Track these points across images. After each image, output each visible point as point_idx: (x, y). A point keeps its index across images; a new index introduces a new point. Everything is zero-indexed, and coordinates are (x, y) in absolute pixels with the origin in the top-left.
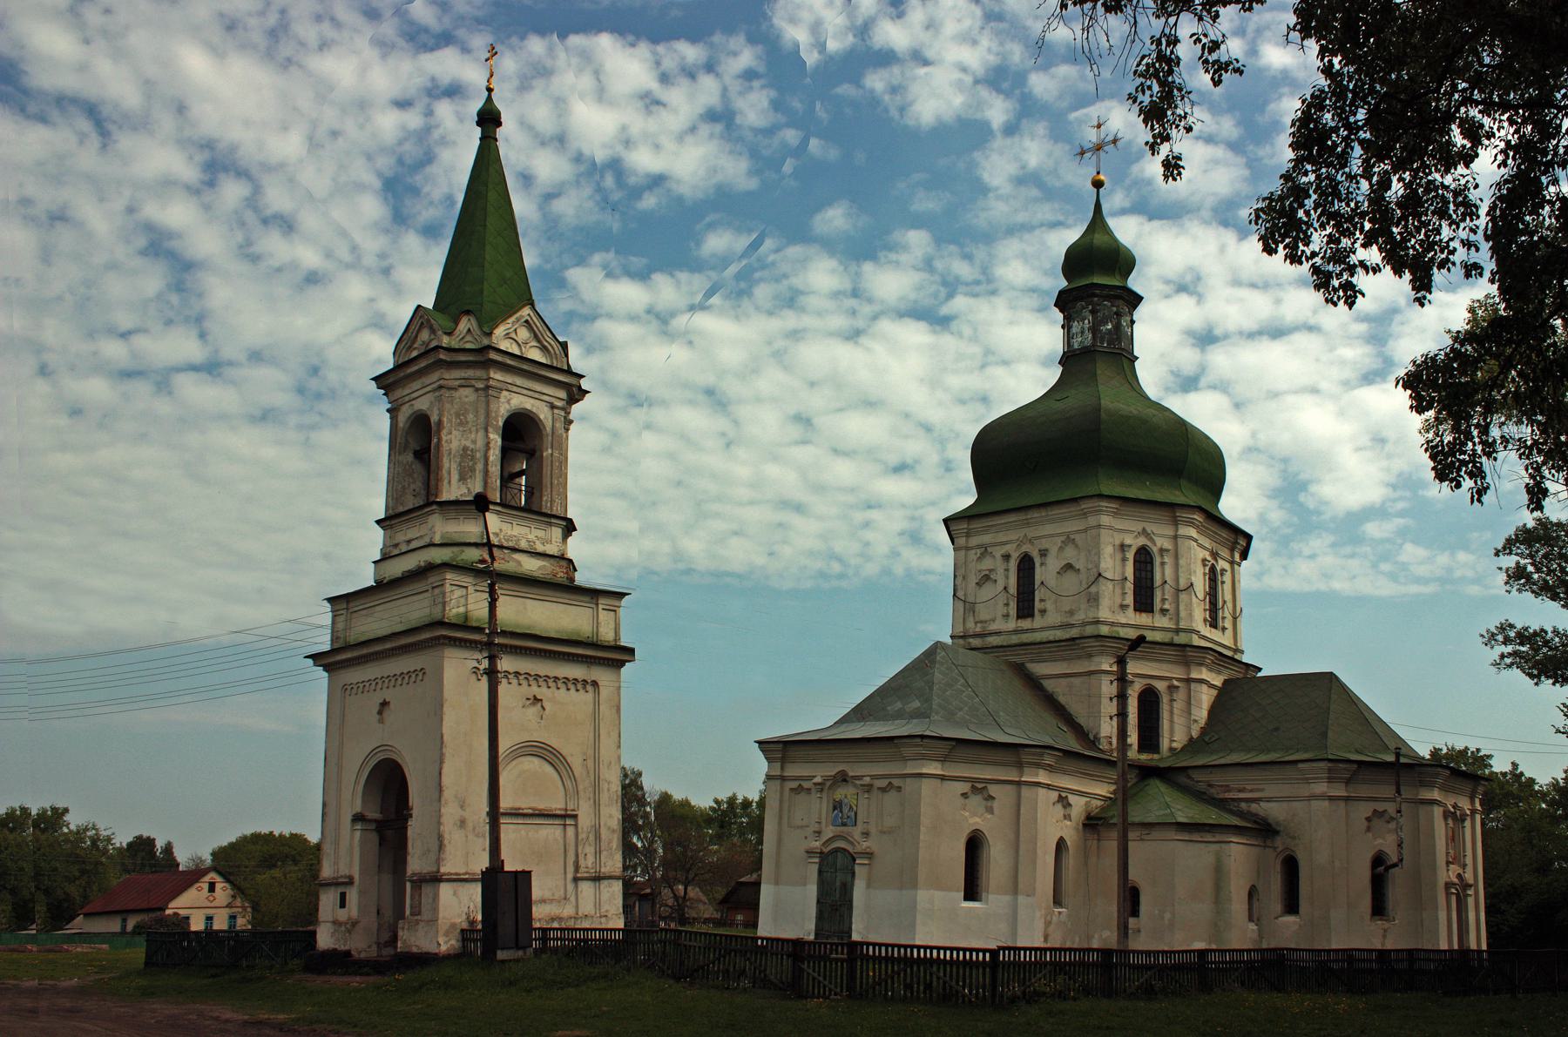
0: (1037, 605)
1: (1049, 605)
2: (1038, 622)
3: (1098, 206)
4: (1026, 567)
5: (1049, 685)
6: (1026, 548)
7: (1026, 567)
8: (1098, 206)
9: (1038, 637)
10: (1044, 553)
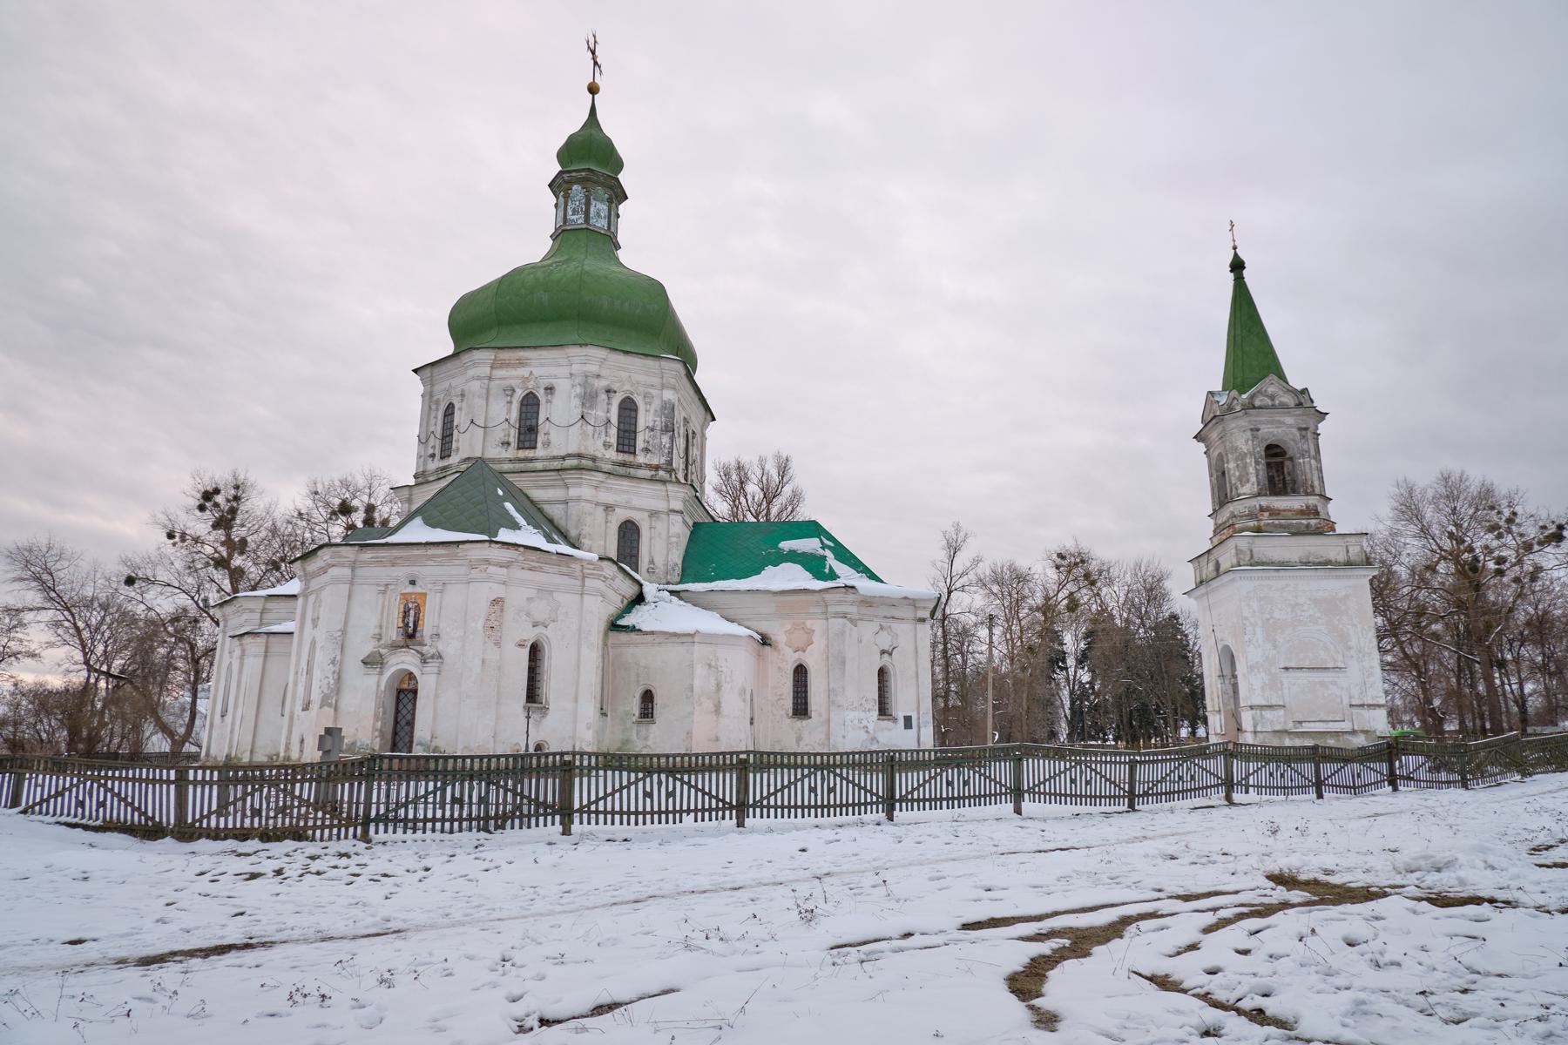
0: (541, 439)
1: (553, 437)
2: (540, 452)
3: (593, 109)
4: (530, 405)
5: (556, 511)
6: (531, 385)
7: (530, 405)
8: (593, 109)
9: (539, 465)
10: (550, 390)
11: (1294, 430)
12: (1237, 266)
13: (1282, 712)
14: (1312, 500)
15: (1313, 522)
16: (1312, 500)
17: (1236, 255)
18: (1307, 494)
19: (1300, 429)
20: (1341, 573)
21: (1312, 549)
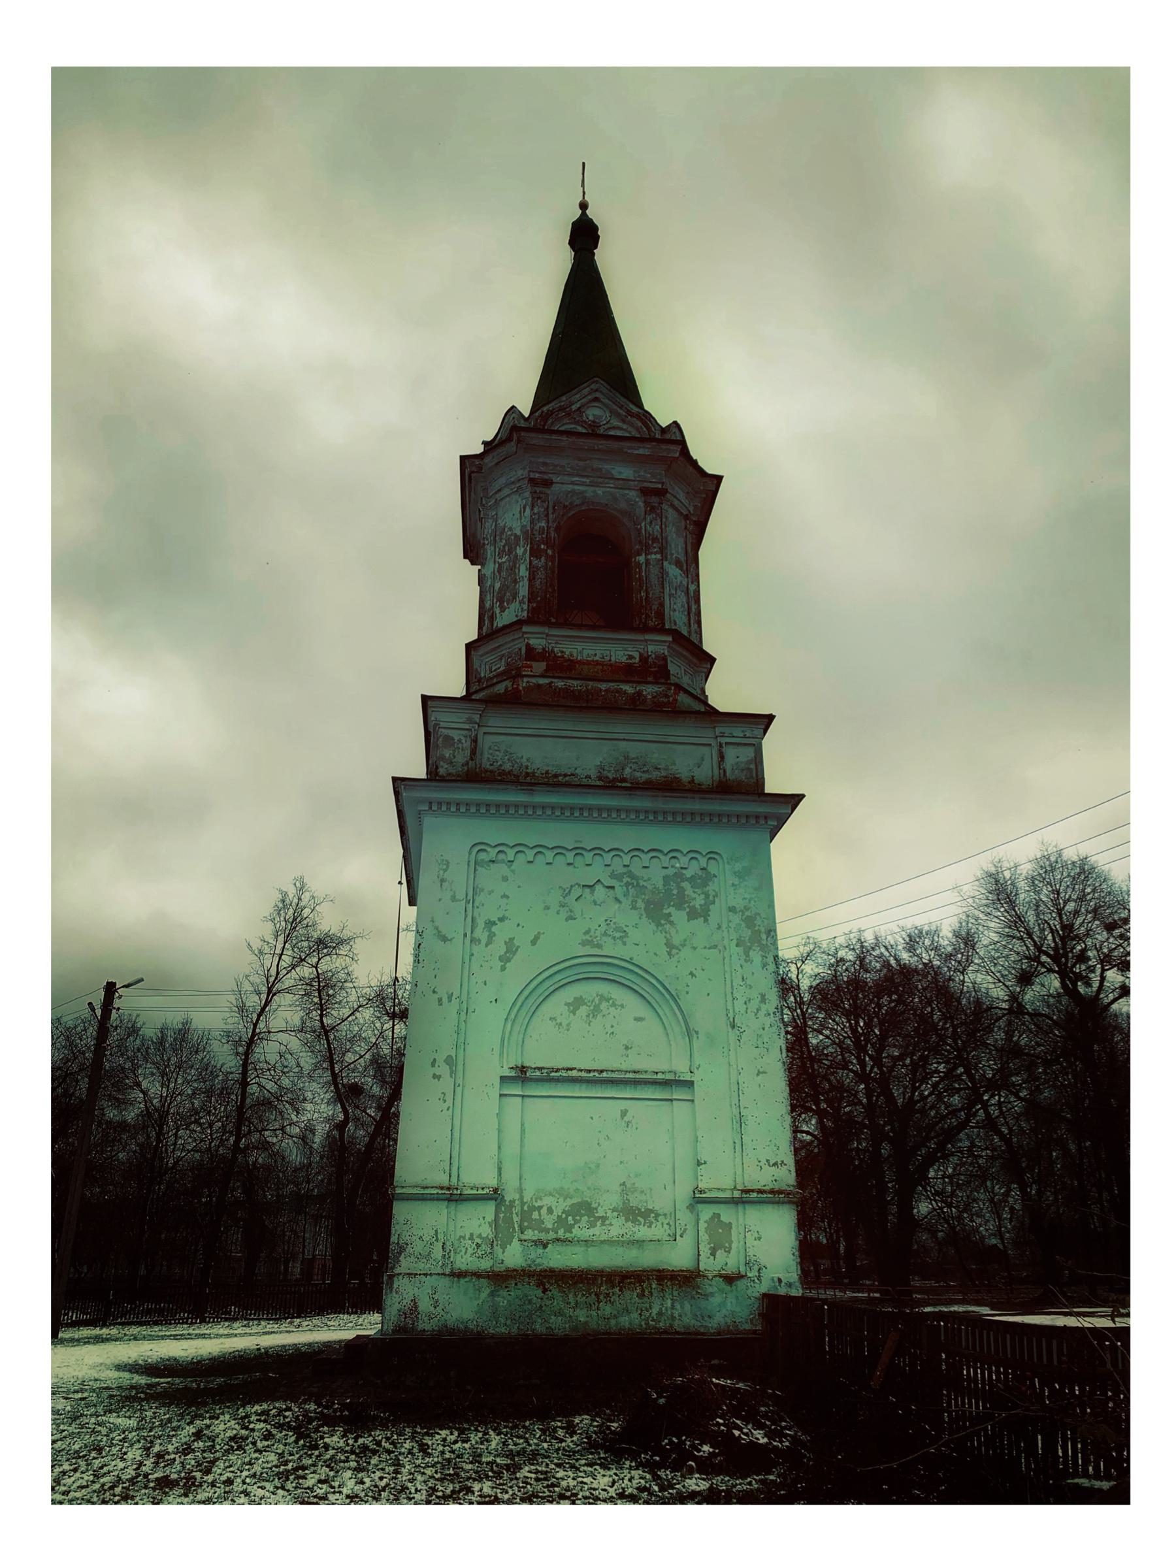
11: (632, 494)
12: (584, 235)
13: (488, 1210)
14: (657, 645)
15: (649, 690)
16: (657, 645)
17: (584, 214)
18: (646, 629)
19: (645, 492)
20: (697, 805)
21: (634, 749)
